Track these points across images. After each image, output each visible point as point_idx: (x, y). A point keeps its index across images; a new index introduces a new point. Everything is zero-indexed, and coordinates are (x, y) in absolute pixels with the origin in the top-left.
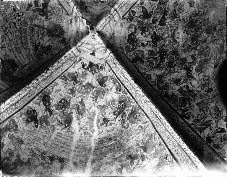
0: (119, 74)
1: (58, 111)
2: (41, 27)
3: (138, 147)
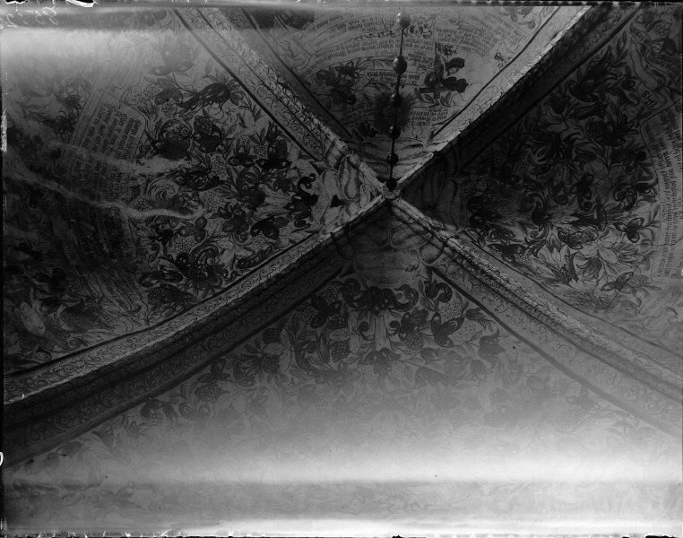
0: (281, 261)
1: (192, 122)
2: (399, 79)
3: (84, 299)
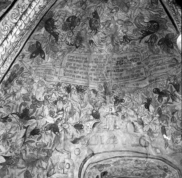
3: (169, 82)
